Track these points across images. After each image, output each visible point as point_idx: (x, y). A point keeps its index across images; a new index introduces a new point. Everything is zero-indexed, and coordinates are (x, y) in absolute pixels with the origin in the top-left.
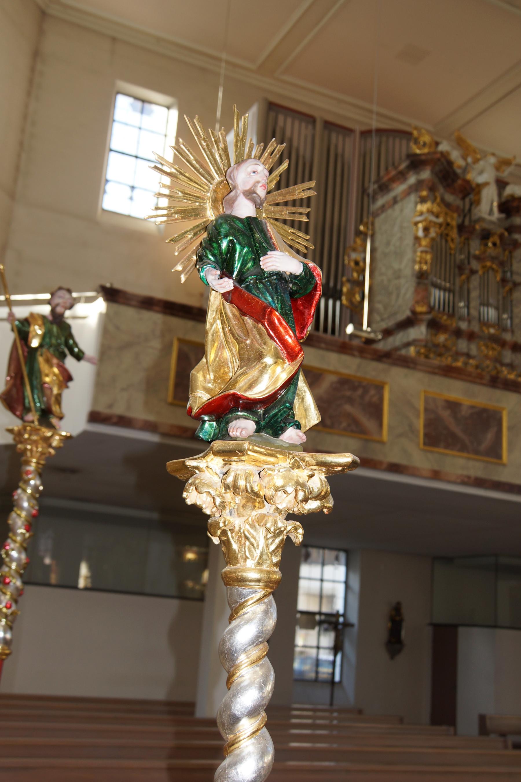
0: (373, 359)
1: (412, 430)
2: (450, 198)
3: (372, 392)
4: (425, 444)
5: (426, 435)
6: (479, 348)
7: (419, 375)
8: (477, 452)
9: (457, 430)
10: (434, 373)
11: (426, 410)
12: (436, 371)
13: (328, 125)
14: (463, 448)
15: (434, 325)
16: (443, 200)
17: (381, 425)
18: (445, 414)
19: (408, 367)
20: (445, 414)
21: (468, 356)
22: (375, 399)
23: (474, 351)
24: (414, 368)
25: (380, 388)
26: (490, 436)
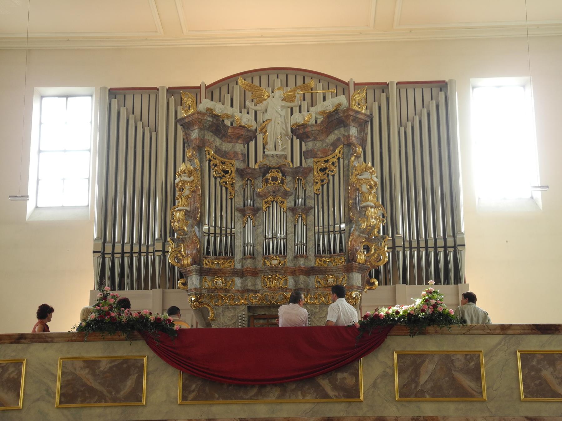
0: (12, 343)
1: (51, 394)
2: (226, 147)
3: (11, 369)
4: (61, 403)
5: (62, 395)
6: (264, 283)
7: (57, 346)
8: (115, 400)
9: (96, 385)
10: (72, 341)
11: (63, 373)
12: (74, 338)
13: (171, 91)
14: (101, 398)
15: (202, 272)
16: (218, 151)
17: (18, 396)
18: (84, 374)
19: (47, 342)
20: (84, 374)
21: (255, 292)
22: (14, 375)
23: (259, 286)
24: (52, 341)
25: (18, 365)
26: (130, 383)
